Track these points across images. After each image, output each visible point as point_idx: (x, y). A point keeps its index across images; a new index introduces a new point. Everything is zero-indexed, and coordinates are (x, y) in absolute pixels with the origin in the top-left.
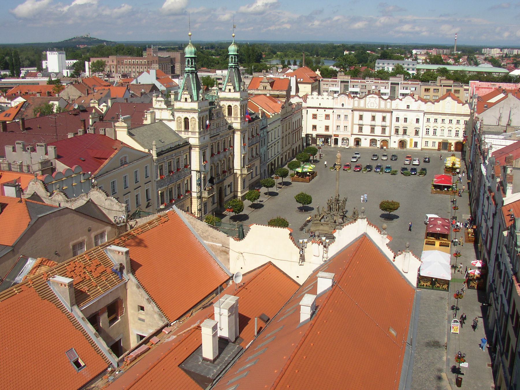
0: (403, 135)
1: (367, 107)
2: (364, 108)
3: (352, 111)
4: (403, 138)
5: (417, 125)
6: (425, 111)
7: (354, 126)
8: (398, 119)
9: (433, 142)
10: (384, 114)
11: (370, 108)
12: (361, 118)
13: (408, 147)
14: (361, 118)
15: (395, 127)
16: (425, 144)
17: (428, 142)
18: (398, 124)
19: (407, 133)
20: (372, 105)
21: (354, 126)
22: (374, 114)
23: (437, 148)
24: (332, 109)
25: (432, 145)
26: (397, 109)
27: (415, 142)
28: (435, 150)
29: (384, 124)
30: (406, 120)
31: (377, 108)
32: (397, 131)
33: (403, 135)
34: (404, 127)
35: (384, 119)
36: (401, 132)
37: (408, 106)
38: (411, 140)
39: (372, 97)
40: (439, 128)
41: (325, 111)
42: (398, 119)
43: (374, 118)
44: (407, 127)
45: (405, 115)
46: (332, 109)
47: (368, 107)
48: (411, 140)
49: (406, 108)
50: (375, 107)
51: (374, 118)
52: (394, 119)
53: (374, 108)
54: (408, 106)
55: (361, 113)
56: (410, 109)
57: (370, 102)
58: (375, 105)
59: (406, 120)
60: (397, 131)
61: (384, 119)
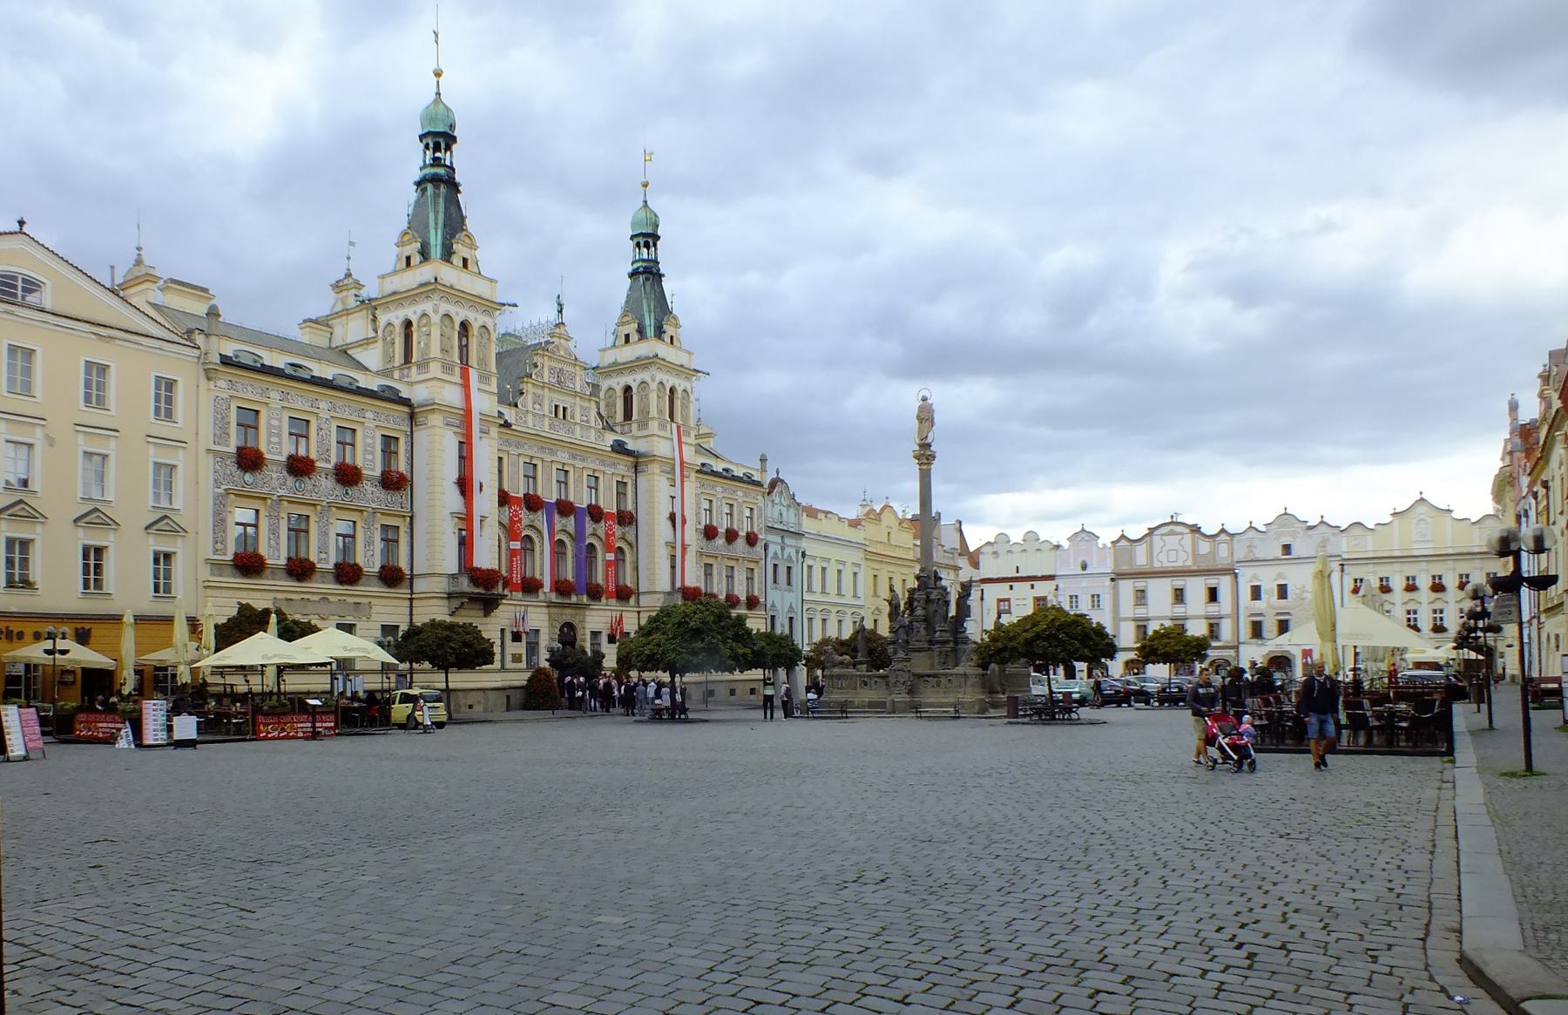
1: (1157, 565)
2: (1148, 569)
3: (1112, 580)
6: (1345, 556)
7: (1122, 623)
8: (1256, 593)
10: (1212, 582)
11: (1166, 564)
12: (1141, 596)
14: (1141, 596)
15: (1252, 615)
18: (1259, 605)
20: (1172, 556)
21: (1122, 623)
22: (1179, 583)
24: (1051, 578)
26: (1251, 561)
29: (1213, 609)
31: (1189, 563)
32: (1257, 630)
34: (1278, 614)
35: (1213, 595)
36: (1270, 627)
37: (1287, 549)
39: (1173, 533)
41: (1032, 587)
42: (1256, 593)
43: (1179, 596)
44: (1288, 614)
45: (1280, 576)
46: (1051, 578)
47: (1162, 562)
49: (1279, 553)
50: (1184, 560)
51: (1179, 596)
52: (1245, 593)
53: (1180, 564)
54: (1287, 549)
55: (1140, 584)
56: (1295, 552)
57: (1165, 549)
58: (1183, 556)
60: (1257, 630)
61: (1213, 595)
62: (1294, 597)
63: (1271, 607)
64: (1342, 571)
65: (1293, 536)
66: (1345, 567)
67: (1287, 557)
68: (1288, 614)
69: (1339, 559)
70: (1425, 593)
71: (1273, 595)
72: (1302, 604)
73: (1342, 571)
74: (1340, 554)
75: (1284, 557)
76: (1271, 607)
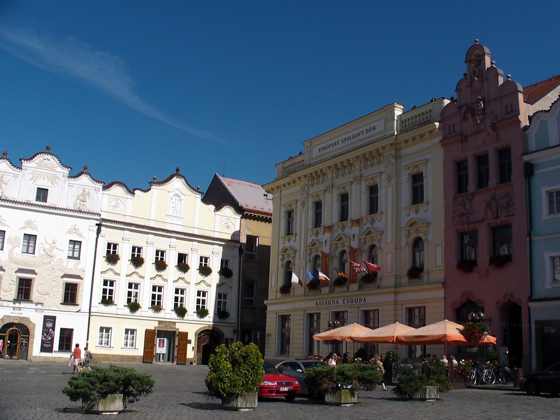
0: (16, 301)
4: (16, 313)
5: (71, 266)
6: (104, 216)
9: (127, 331)
13: (35, 349)
16: (98, 340)
17: (108, 330)
19: (35, 295)
23: (139, 351)
25: (123, 341)
27: (62, 330)
28: (134, 358)
30: (30, 238)
33: (16, 301)
34: (20, 270)
37: (42, 194)
38: (50, 320)
40: (147, 278)
44: (33, 272)
45: (29, 223)
48: (50, 320)
49: (32, 197)
54: (42, 194)
56: (50, 201)
59: (30, 238)
62: (42, 252)
63: (12, 260)
64: (99, 231)
65: (54, 179)
66: (103, 228)
67: (39, 203)
68: (33, 272)
69: (98, 217)
70: (194, 273)
71: (19, 247)
72: (50, 262)
73: (99, 231)
74: (99, 212)
75: (37, 203)
76: (12, 260)
